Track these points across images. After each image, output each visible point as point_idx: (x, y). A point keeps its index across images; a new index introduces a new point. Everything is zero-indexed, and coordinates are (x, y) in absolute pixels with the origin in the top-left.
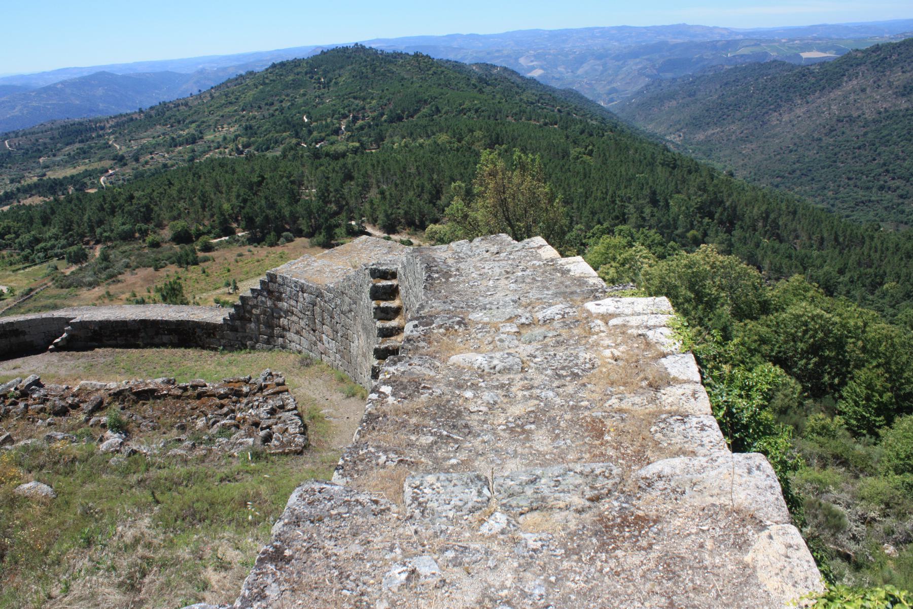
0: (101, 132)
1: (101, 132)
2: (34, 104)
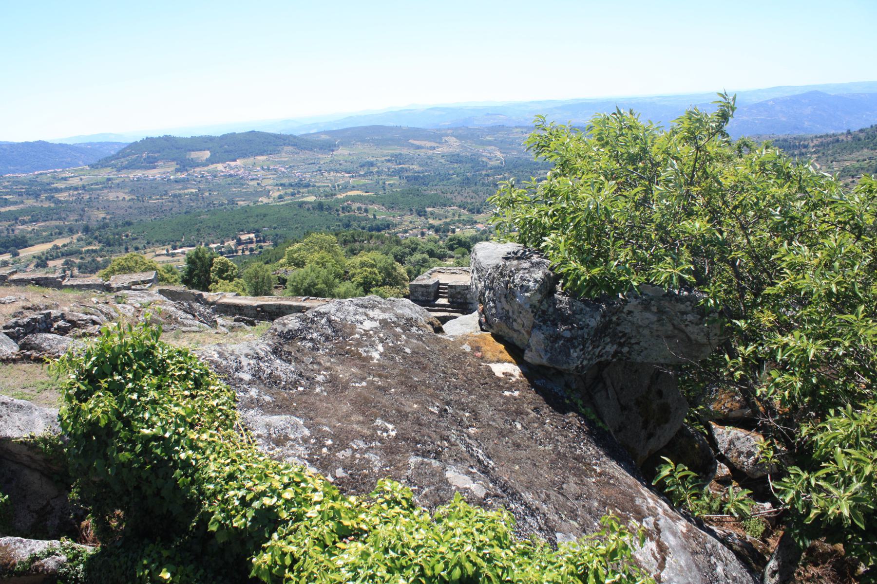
0: (803, 150)
1: (803, 150)
2: (745, 118)
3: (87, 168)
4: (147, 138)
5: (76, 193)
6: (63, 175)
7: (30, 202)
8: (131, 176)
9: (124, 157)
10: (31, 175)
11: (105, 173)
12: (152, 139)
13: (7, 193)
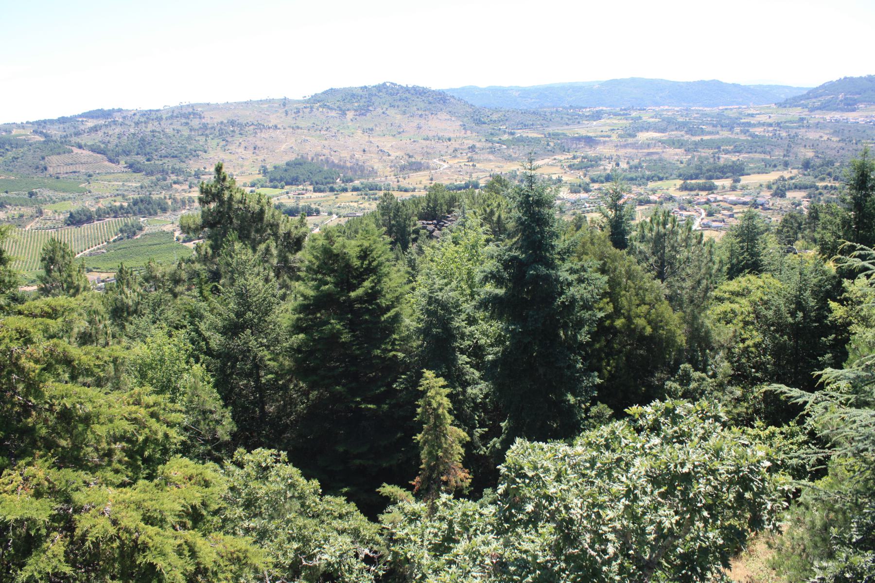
3: (773, 106)
4: (845, 78)
5: (771, 129)
6: (749, 112)
7: (725, 134)
8: (828, 117)
9: (816, 97)
10: (716, 110)
11: (795, 113)
12: (851, 79)
13: (702, 124)
